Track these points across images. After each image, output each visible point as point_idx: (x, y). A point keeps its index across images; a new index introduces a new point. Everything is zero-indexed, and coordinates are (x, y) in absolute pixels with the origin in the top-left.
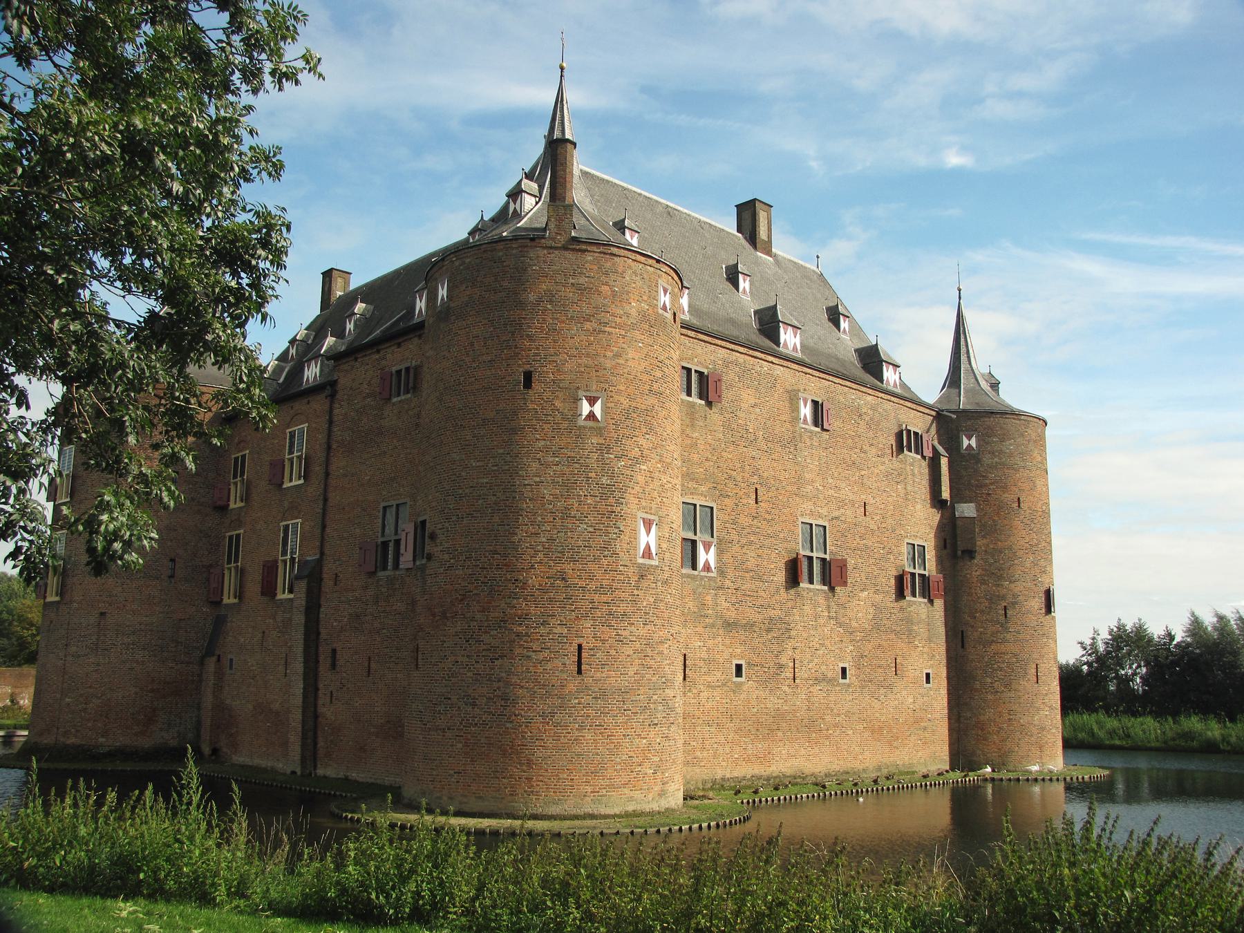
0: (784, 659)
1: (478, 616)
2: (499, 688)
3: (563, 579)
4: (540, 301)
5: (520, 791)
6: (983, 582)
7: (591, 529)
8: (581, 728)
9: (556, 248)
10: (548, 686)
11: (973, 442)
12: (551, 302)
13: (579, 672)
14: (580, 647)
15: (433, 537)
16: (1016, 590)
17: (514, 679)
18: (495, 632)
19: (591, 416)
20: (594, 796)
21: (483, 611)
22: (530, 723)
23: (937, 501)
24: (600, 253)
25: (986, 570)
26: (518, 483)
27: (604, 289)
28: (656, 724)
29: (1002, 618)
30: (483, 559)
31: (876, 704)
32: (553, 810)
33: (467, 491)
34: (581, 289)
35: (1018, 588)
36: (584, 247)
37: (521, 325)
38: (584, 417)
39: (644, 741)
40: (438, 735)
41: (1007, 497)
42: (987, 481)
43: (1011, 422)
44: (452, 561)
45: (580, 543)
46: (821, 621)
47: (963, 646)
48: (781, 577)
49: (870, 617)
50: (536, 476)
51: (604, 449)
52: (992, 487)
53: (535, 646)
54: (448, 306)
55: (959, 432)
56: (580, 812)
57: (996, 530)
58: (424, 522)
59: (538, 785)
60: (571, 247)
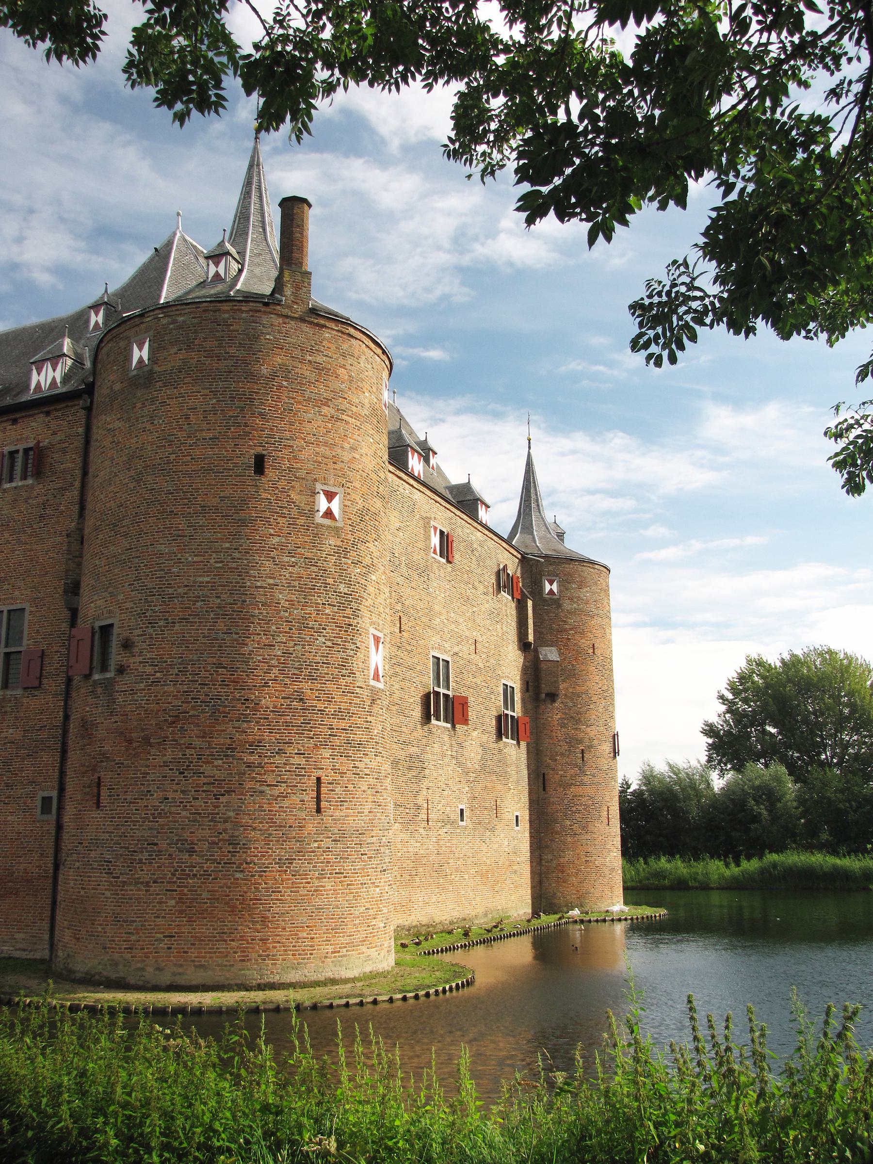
0: (420, 801)
1: (197, 742)
2: (225, 830)
3: (301, 700)
4: (273, 376)
5: (254, 956)
6: (563, 726)
7: (329, 644)
8: (321, 877)
9: (292, 318)
10: (285, 827)
11: (555, 587)
12: (286, 378)
13: (319, 810)
14: (319, 779)
15: (127, 645)
16: (592, 734)
17: (245, 820)
18: (220, 762)
19: (329, 514)
20: (335, 957)
21: (203, 737)
22: (265, 872)
23: (524, 646)
24: (338, 331)
25: (565, 714)
26: (248, 584)
27: (341, 371)
28: (385, 871)
29: (580, 761)
30: (203, 673)
31: (484, 848)
32: (292, 976)
33: (180, 590)
34: (319, 369)
35: (592, 731)
36: (322, 322)
37: (252, 400)
38: (321, 514)
39: (377, 889)
40: (139, 890)
41: (584, 643)
42: (567, 626)
43: (587, 570)
44: (158, 675)
45: (318, 659)
46: (447, 760)
47: (544, 789)
48: (417, 713)
49: (479, 757)
50: (270, 578)
51: (342, 552)
52: (571, 632)
53: (270, 779)
54: (151, 370)
55: (541, 576)
56: (321, 977)
57: (574, 675)
58: (106, 630)
59: (275, 947)
60: (307, 319)
